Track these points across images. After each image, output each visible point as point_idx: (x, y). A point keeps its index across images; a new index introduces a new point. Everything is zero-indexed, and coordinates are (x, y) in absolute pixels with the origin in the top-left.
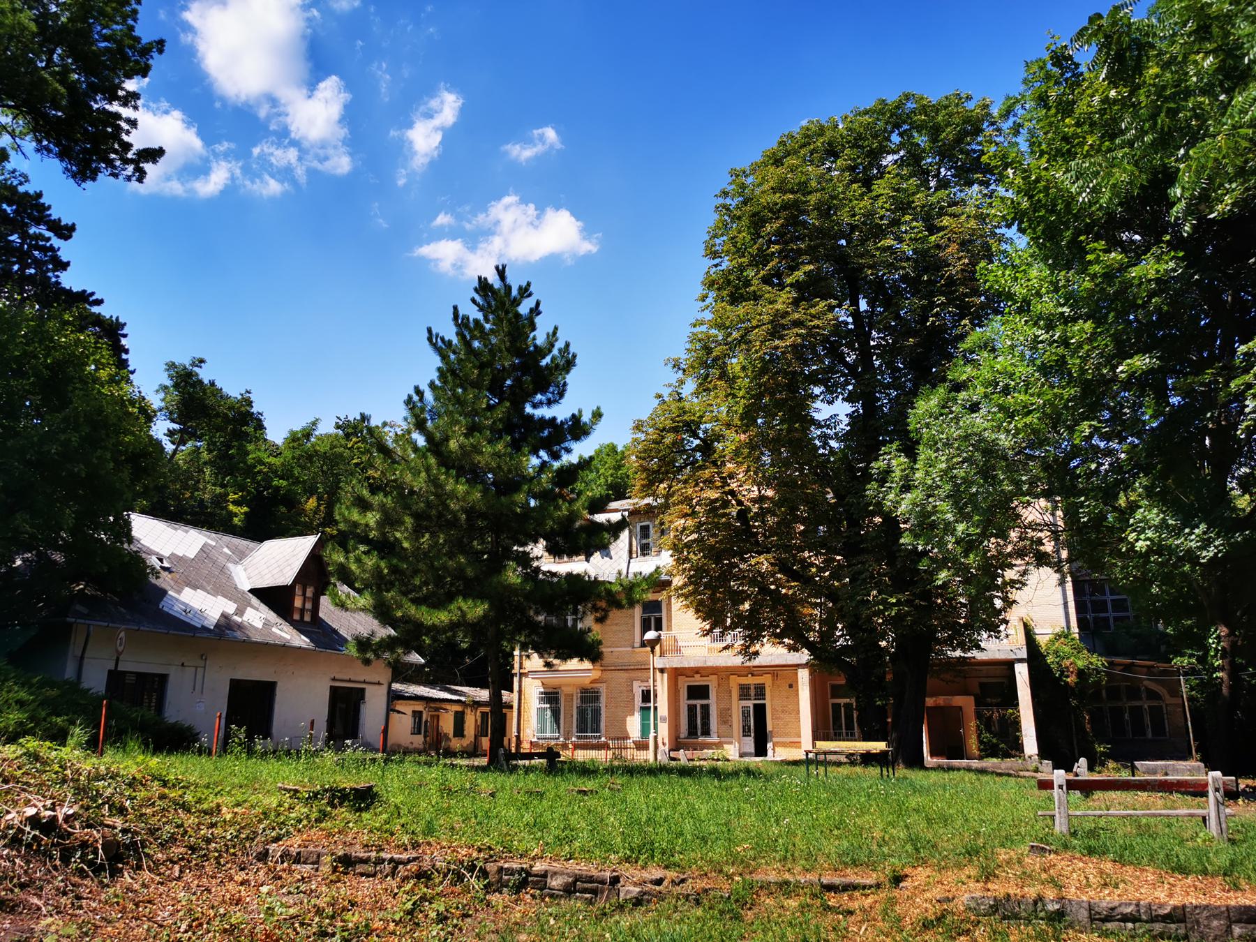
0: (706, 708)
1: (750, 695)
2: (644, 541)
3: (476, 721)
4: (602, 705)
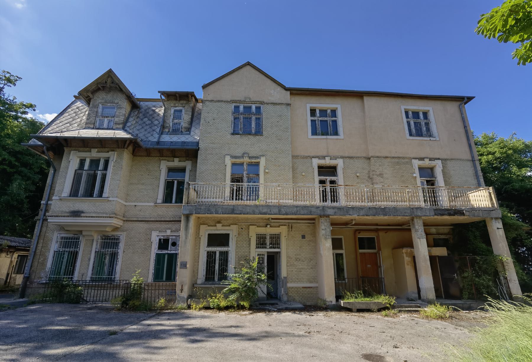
0: (225, 256)
1: (265, 244)
2: (176, 121)
3: (11, 262)
4: (120, 252)
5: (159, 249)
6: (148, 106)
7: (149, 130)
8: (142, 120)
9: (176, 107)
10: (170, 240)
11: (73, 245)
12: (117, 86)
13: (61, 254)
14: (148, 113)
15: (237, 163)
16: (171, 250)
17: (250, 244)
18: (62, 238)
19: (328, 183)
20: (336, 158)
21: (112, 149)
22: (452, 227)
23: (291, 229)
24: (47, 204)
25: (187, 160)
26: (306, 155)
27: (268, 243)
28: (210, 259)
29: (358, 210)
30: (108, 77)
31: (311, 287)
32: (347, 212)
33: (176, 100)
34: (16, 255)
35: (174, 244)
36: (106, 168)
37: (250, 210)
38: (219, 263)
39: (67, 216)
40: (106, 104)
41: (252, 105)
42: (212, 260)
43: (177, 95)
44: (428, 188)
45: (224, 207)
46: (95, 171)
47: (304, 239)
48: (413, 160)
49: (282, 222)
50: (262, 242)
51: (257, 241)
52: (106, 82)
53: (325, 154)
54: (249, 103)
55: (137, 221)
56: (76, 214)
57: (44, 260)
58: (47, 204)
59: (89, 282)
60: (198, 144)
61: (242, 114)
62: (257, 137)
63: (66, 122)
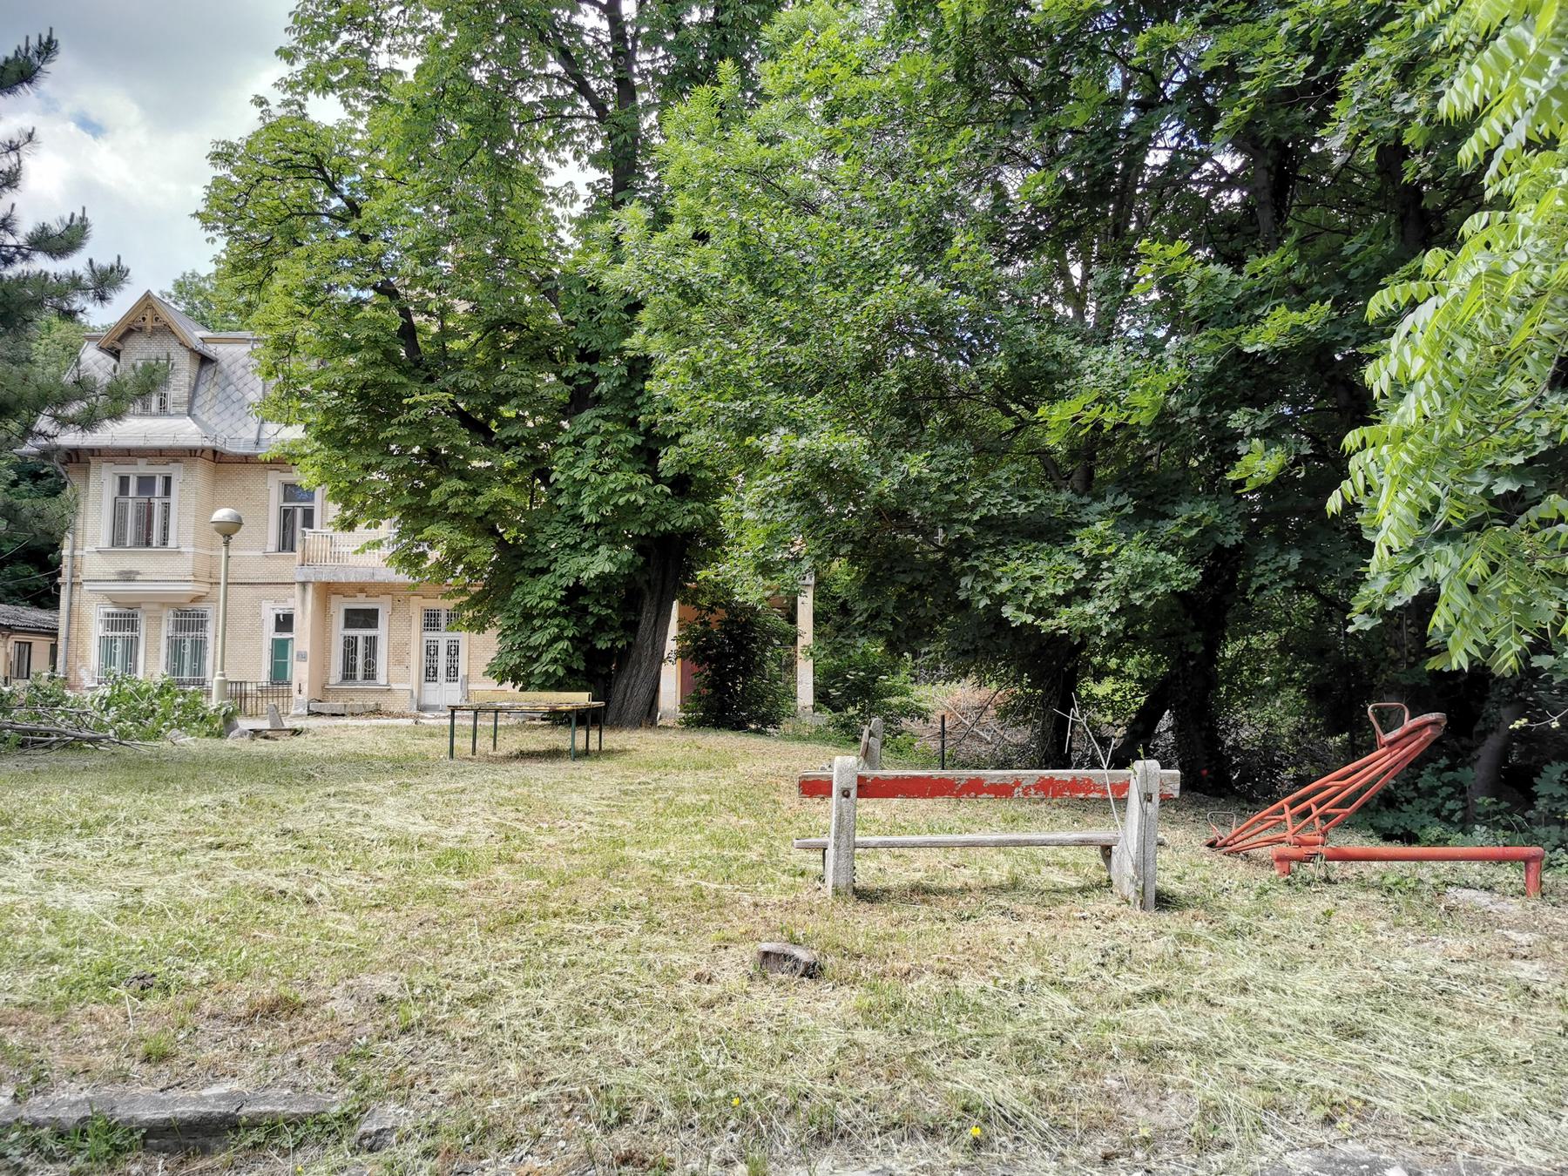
0: (371, 642)
3: (7, 655)
34: (11, 643)
36: (167, 491)
56: (128, 576)
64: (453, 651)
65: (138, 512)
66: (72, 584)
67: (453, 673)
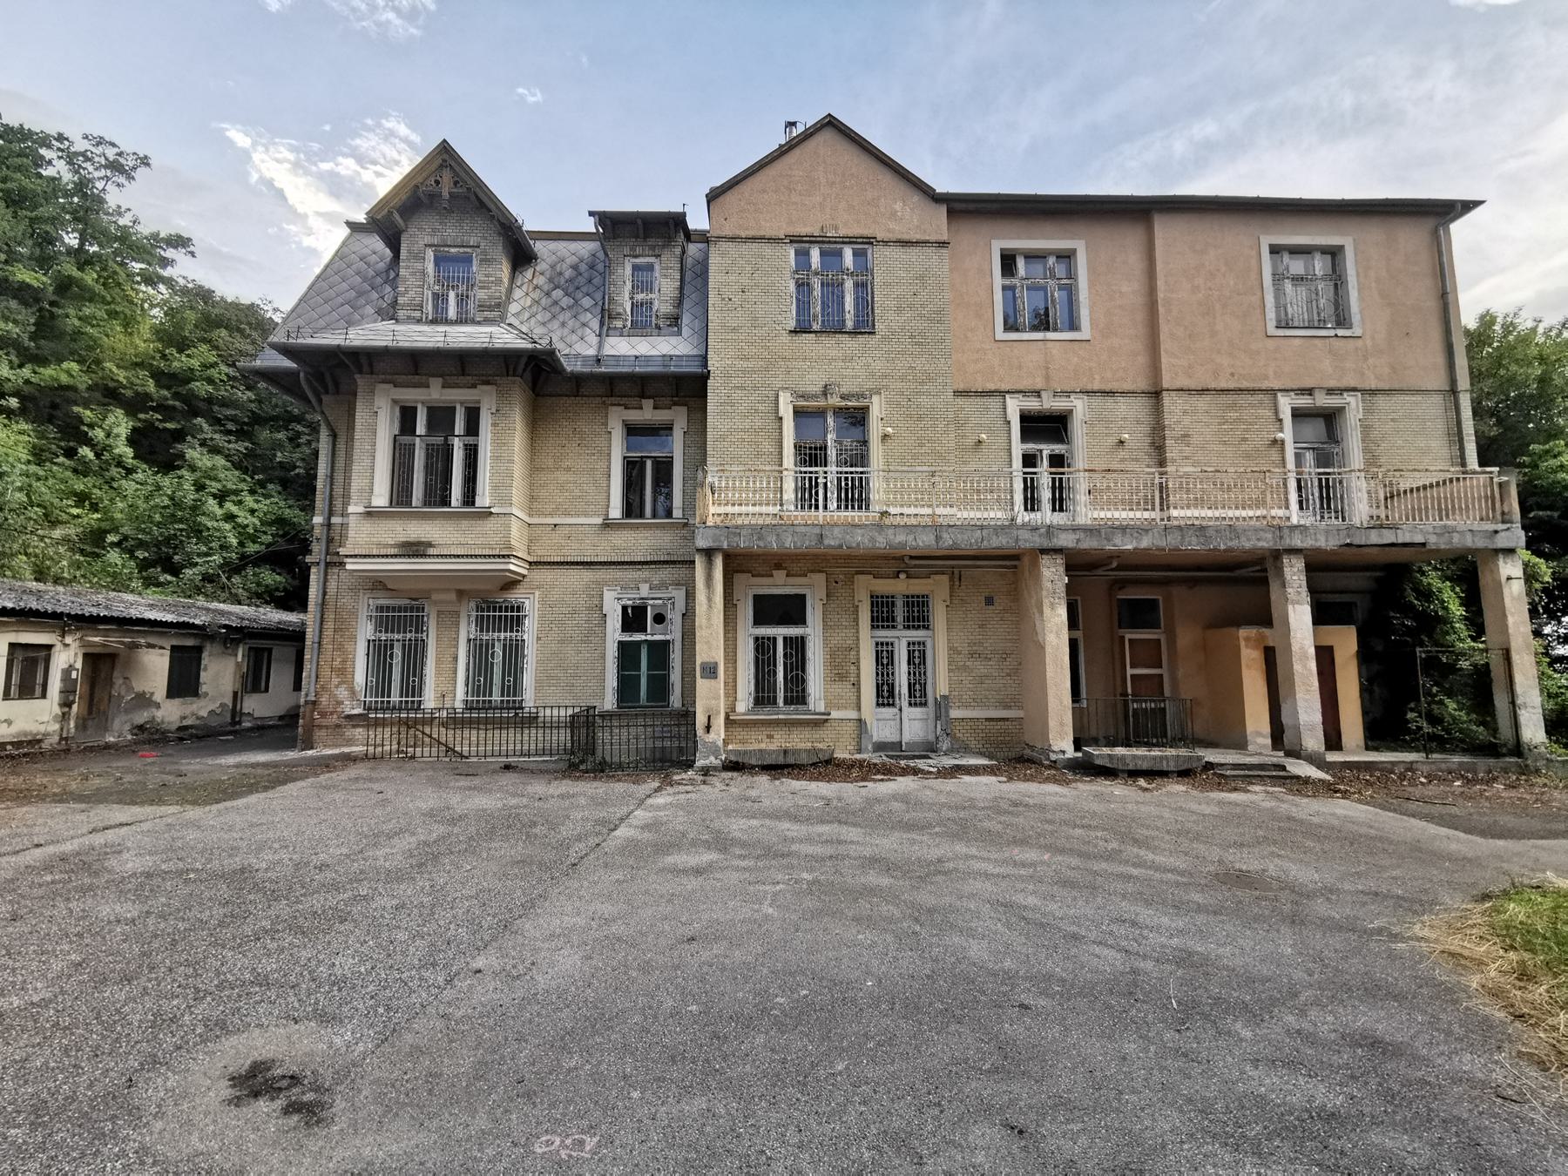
0: (797, 647)
2: (640, 297)
5: (624, 630)
6: (559, 254)
7: (571, 323)
8: (548, 294)
9: (636, 257)
10: (649, 608)
11: (411, 626)
12: (473, 198)
13: (386, 645)
14: (561, 274)
15: (809, 410)
16: (653, 634)
17: (858, 618)
18: (380, 609)
19: (1046, 462)
20: (1067, 394)
21: (484, 378)
22: (1378, 574)
23: (957, 583)
24: (328, 525)
25: (675, 404)
26: (991, 386)
27: (900, 619)
28: (763, 654)
29: (1135, 535)
30: (441, 166)
31: (1007, 719)
32: (1108, 540)
33: (637, 237)
35: (659, 619)
36: (472, 428)
37: (863, 536)
38: (785, 664)
39: (392, 556)
40: (446, 249)
41: (842, 246)
42: (769, 658)
43: (639, 222)
44: (1319, 474)
45: (798, 529)
46: (446, 440)
47: (991, 607)
48: (1279, 394)
49: (932, 566)
50: (885, 615)
51: (872, 612)
52: (437, 182)
53: (1039, 383)
54: (835, 242)
55: (562, 563)
56: (415, 549)
57: (344, 661)
58: (328, 525)
59: (463, 713)
60: (707, 361)
61: (817, 274)
62: (861, 338)
63: (340, 300)
64: (918, 658)
65: (428, 456)
66: (328, 564)
67: (918, 694)
